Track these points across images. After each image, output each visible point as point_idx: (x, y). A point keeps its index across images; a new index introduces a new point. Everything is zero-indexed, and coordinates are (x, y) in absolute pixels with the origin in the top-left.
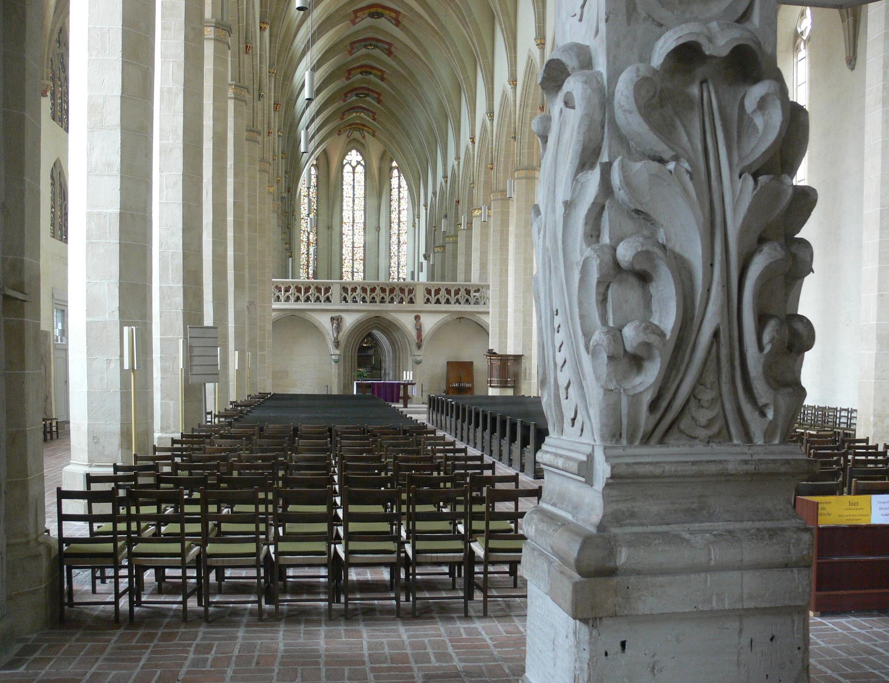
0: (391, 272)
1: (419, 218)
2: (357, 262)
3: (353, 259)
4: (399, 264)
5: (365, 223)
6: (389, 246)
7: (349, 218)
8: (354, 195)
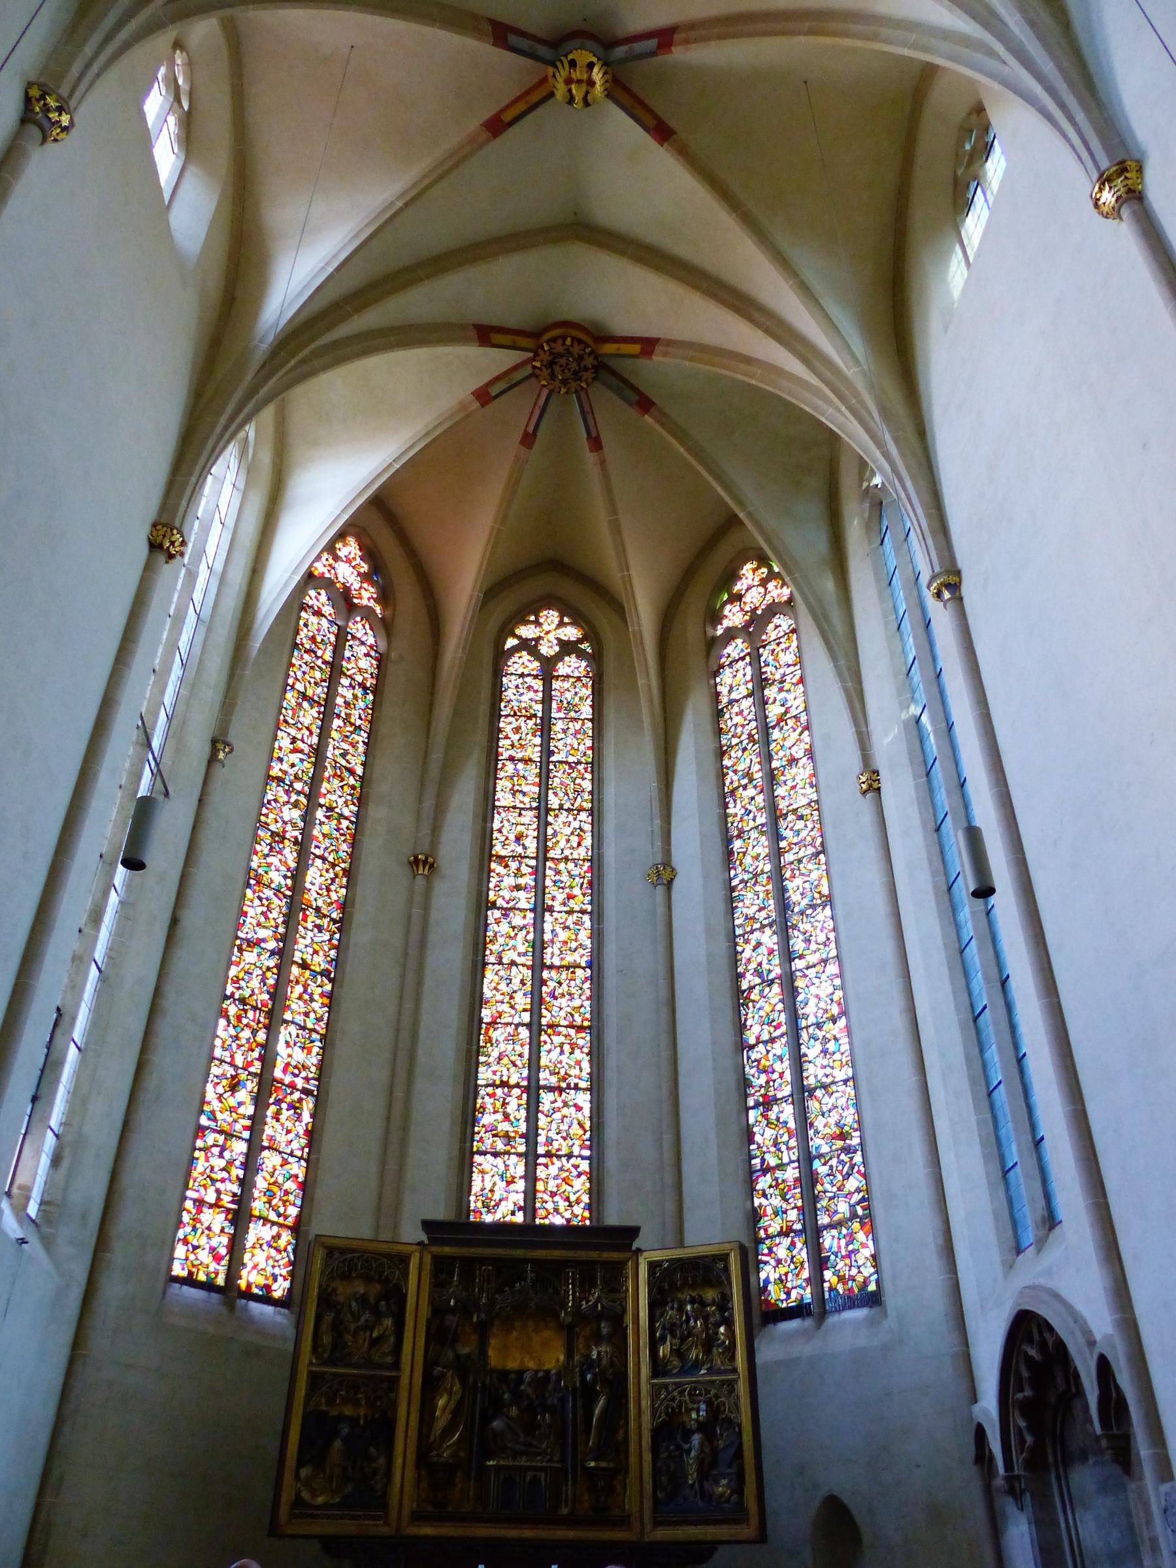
0: (750, 1071)
2: (557, 1040)
3: (535, 1028)
4: (794, 1017)
5: (596, 862)
6: (723, 945)
7: (519, 838)
8: (547, 752)
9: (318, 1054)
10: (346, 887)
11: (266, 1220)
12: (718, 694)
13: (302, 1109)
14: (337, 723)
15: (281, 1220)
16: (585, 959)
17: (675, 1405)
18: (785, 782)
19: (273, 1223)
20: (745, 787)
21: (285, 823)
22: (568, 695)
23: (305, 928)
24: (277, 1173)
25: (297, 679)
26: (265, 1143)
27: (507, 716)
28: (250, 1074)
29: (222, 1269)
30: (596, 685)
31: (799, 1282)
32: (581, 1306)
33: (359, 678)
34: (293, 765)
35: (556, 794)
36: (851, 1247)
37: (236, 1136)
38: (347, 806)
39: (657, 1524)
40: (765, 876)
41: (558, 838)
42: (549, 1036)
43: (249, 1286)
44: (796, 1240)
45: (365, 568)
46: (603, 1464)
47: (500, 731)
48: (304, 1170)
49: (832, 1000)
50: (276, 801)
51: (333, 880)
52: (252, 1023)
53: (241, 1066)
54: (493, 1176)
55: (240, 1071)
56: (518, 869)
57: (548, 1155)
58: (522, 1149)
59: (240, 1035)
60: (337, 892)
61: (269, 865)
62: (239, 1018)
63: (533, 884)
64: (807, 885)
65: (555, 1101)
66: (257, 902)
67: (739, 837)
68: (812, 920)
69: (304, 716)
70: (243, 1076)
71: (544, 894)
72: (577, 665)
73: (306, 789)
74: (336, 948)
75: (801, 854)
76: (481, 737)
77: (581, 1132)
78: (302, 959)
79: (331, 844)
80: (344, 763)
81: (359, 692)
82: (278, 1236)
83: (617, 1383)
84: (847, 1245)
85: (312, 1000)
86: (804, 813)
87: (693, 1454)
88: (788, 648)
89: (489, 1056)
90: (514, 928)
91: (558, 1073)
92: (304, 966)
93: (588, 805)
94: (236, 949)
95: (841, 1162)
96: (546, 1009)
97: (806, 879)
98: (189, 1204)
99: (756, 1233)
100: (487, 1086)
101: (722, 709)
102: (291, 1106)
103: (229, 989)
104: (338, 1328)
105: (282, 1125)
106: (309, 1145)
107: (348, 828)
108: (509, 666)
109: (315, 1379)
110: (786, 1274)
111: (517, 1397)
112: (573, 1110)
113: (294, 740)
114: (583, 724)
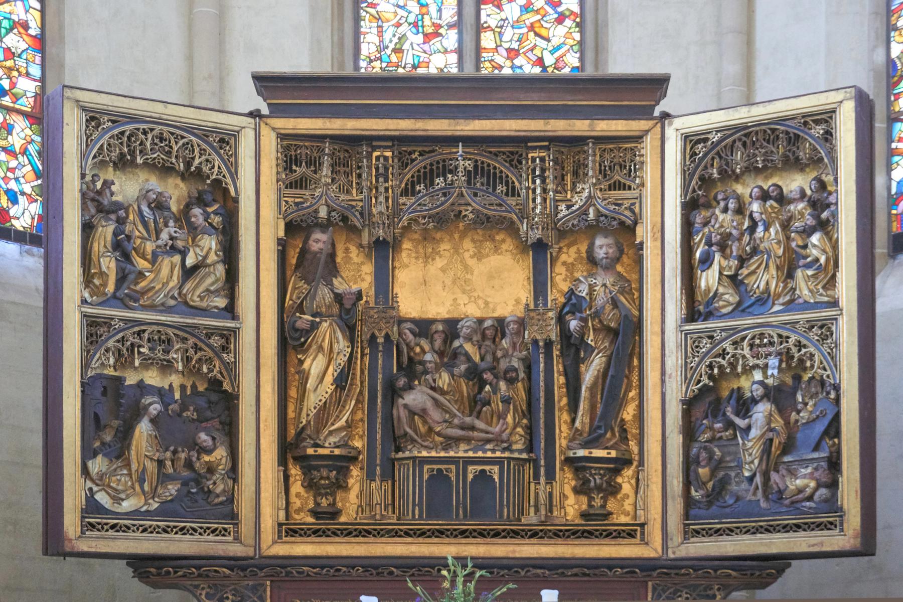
17: (724, 362)
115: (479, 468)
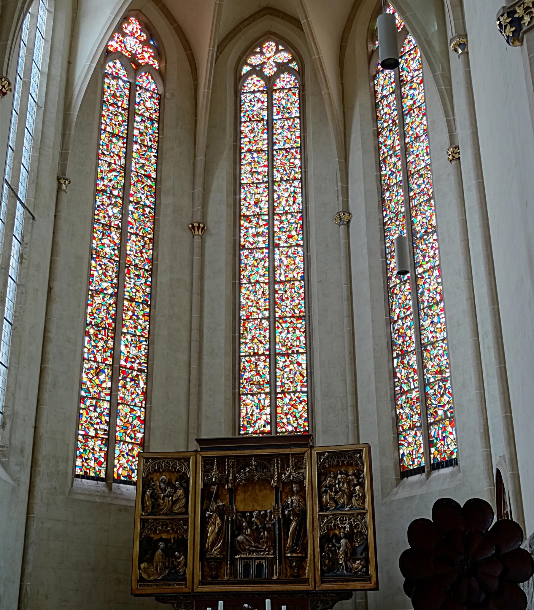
1: (463, 46)
3: (273, 320)
4: (417, 303)
5: (305, 213)
8: (271, 143)
9: (145, 349)
10: (152, 249)
11: (125, 442)
12: (376, 92)
13: (139, 381)
14: (136, 147)
15: (133, 441)
16: (300, 275)
18: (413, 151)
19: (129, 443)
20: (391, 156)
21: (110, 217)
22: (284, 102)
23: (130, 278)
24: (128, 416)
25: (107, 125)
26: (120, 401)
27: (245, 122)
28: (106, 365)
29: (103, 468)
30: (301, 93)
31: (419, 455)
32: (282, 477)
33: (147, 115)
34: (111, 181)
35: (278, 171)
36: (444, 435)
37: (103, 400)
38: (148, 199)
39: (323, 582)
40: (402, 215)
41: (281, 200)
42: (280, 324)
43: (119, 476)
44: (417, 432)
45: (144, 37)
46: (294, 555)
47: (241, 133)
48: (144, 413)
49: (436, 292)
50: (103, 205)
51: (144, 246)
52: (104, 337)
53: (100, 361)
54: (252, 407)
55: (100, 364)
56: (257, 223)
57: (283, 392)
58: (268, 390)
59: (98, 345)
60: (146, 253)
61: (103, 244)
62: (96, 335)
63: (266, 231)
64: (424, 220)
65: (286, 361)
66: (99, 268)
67: (388, 190)
68: (427, 242)
69: (114, 147)
70: (102, 366)
71: (274, 236)
72: (288, 80)
73: (121, 193)
74: (150, 286)
75: (421, 200)
76: (229, 140)
77: (301, 378)
78: (129, 296)
79: (140, 225)
80: (143, 172)
81: (148, 124)
82: (133, 449)
83: (302, 516)
84: (442, 433)
85: (138, 318)
86: (423, 173)
87: (341, 548)
88: (415, 58)
89: (246, 339)
90: (256, 260)
91: (287, 345)
92: (131, 300)
93: (298, 176)
94: (89, 297)
95: (440, 387)
96: (278, 308)
97: (424, 216)
98: (80, 437)
99: (398, 429)
100: (245, 356)
101: (378, 102)
102: (132, 380)
103: (89, 320)
104: (154, 496)
105: (128, 390)
106: (145, 400)
107: (150, 213)
108: (245, 87)
109: (144, 522)
110: (412, 451)
111: (250, 524)
112: (296, 365)
113: (110, 164)
114: (294, 121)
115: (259, 561)
